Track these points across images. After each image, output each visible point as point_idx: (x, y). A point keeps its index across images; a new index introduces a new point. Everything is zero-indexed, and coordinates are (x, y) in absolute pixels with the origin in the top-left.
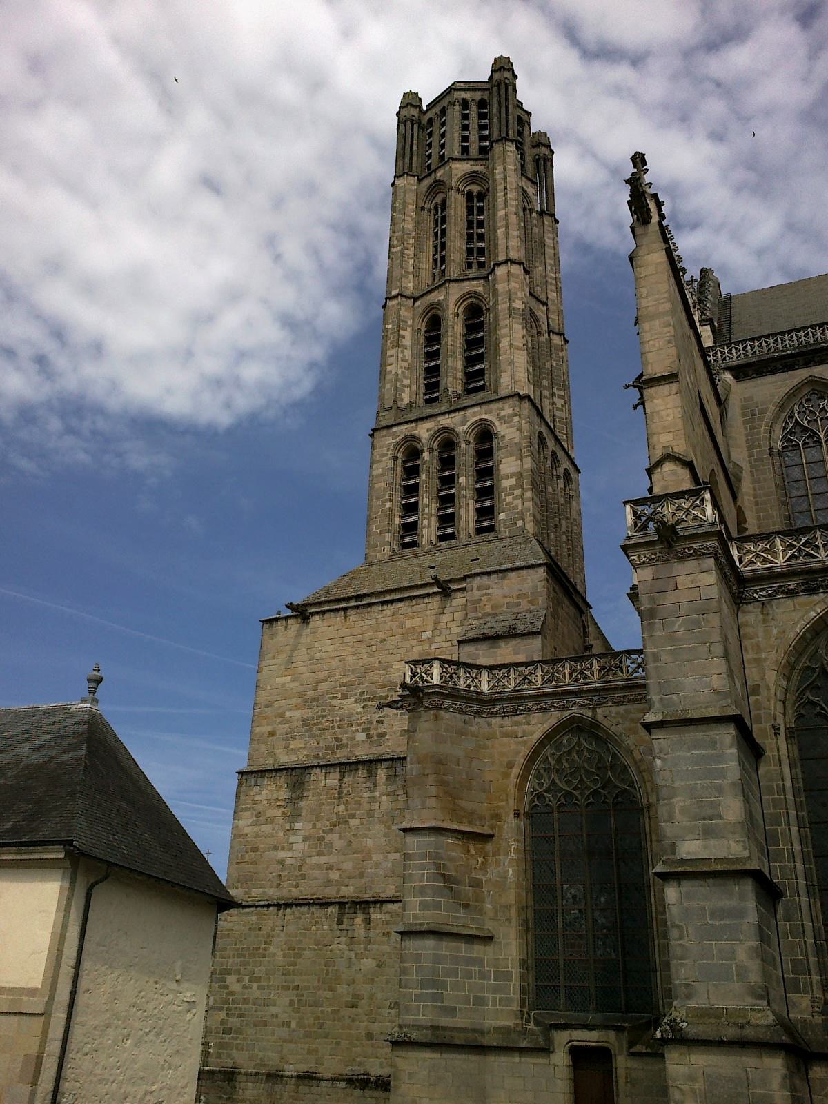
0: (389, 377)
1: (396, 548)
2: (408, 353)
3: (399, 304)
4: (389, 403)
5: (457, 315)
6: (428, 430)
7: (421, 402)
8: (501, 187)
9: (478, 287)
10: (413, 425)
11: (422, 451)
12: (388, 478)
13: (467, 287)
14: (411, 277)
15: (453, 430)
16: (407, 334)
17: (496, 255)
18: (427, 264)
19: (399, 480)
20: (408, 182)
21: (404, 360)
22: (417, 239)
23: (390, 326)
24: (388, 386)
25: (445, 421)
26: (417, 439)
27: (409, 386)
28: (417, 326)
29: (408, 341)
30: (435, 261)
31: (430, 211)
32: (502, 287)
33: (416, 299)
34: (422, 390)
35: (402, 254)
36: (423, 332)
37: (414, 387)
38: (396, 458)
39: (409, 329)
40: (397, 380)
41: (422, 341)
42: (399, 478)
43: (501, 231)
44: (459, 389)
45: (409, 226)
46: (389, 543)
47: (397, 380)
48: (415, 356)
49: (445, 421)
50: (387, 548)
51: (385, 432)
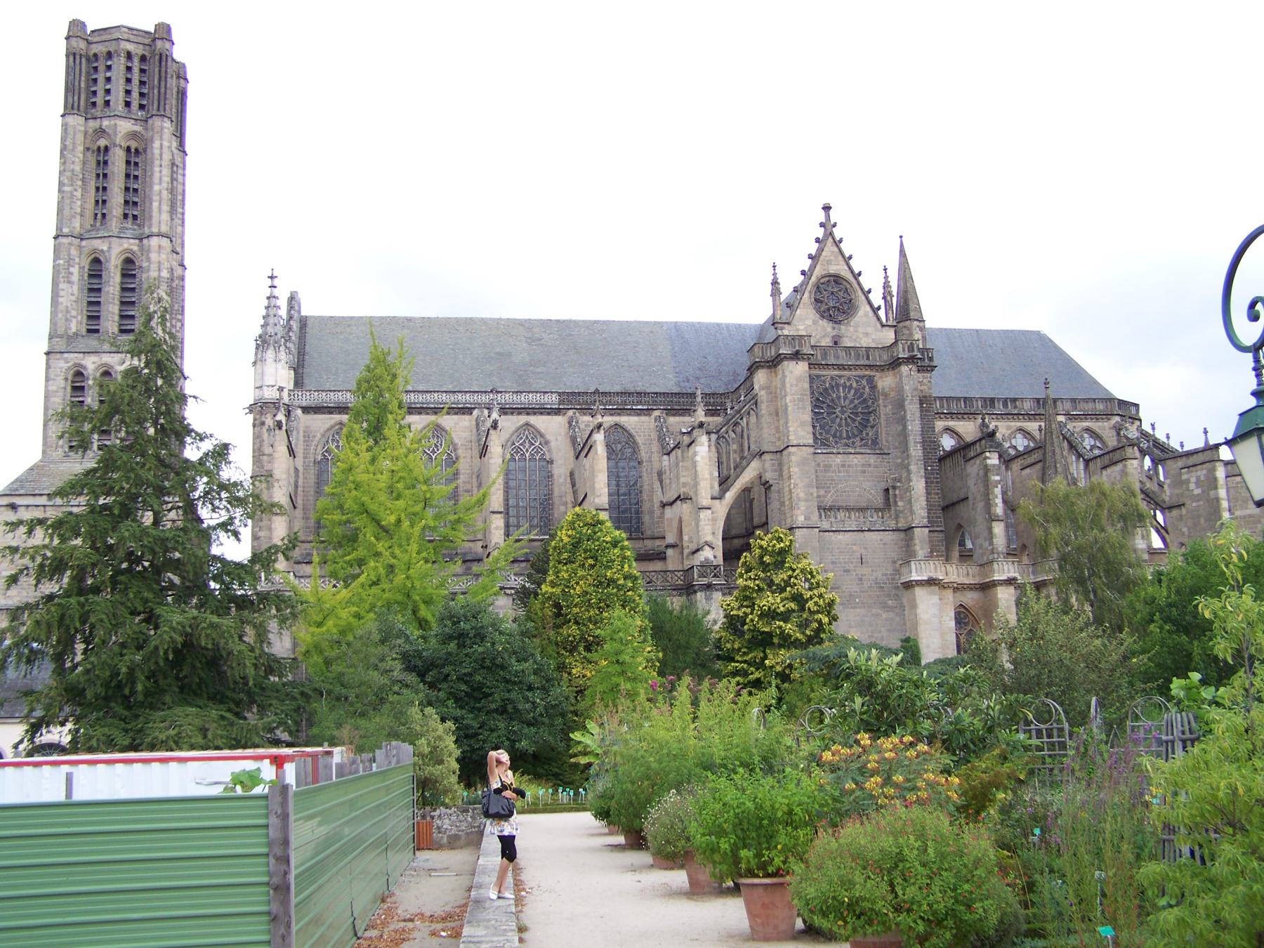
0: (61, 307)
1: (67, 450)
2: (75, 288)
3: (70, 244)
4: (61, 331)
5: (116, 267)
6: (94, 363)
7: (84, 331)
8: (157, 163)
9: (133, 245)
10: (81, 355)
11: (88, 379)
12: (61, 394)
13: (126, 244)
14: (78, 217)
15: (112, 367)
16: (75, 270)
17: (150, 227)
18: (90, 204)
19: (68, 397)
20: (76, 121)
21: (73, 295)
22: (83, 180)
23: (61, 262)
24: (60, 315)
25: (107, 359)
26: (85, 368)
27: (75, 317)
28: (82, 265)
29: (75, 278)
30: (97, 202)
31: (93, 152)
32: (154, 256)
33: (82, 239)
34: (85, 321)
35: (72, 196)
36: (86, 270)
37: (79, 317)
38: (66, 379)
39: (77, 266)
40: (68, 312)
41: (86, 278)
42: (69, 395)
43: (155, 204)
44: (116, 330)
45: (78, 168)
46: (62, 447)
47: (68, 312)
48: (80, 289)
49: (107, 359)
50: (60, 450)
51: (58, 356)
